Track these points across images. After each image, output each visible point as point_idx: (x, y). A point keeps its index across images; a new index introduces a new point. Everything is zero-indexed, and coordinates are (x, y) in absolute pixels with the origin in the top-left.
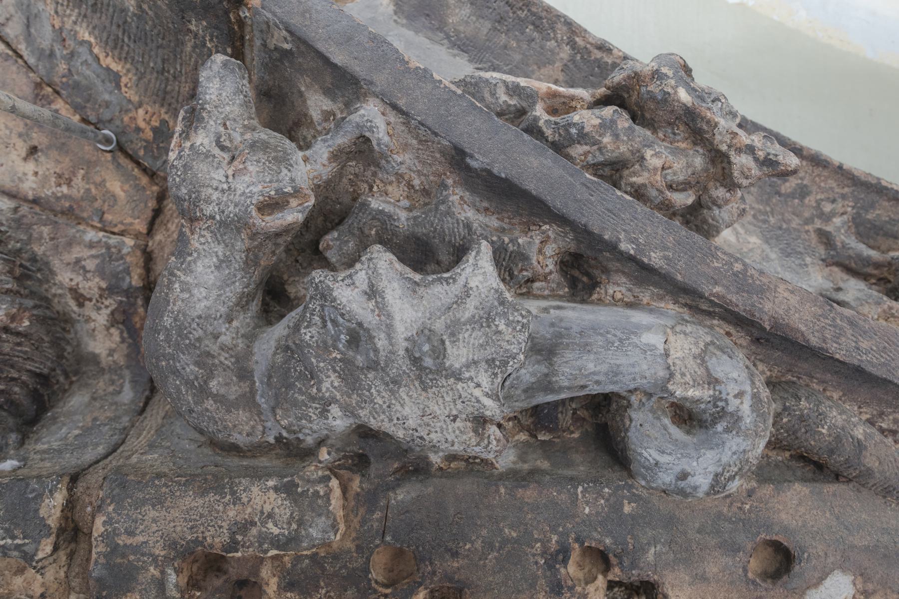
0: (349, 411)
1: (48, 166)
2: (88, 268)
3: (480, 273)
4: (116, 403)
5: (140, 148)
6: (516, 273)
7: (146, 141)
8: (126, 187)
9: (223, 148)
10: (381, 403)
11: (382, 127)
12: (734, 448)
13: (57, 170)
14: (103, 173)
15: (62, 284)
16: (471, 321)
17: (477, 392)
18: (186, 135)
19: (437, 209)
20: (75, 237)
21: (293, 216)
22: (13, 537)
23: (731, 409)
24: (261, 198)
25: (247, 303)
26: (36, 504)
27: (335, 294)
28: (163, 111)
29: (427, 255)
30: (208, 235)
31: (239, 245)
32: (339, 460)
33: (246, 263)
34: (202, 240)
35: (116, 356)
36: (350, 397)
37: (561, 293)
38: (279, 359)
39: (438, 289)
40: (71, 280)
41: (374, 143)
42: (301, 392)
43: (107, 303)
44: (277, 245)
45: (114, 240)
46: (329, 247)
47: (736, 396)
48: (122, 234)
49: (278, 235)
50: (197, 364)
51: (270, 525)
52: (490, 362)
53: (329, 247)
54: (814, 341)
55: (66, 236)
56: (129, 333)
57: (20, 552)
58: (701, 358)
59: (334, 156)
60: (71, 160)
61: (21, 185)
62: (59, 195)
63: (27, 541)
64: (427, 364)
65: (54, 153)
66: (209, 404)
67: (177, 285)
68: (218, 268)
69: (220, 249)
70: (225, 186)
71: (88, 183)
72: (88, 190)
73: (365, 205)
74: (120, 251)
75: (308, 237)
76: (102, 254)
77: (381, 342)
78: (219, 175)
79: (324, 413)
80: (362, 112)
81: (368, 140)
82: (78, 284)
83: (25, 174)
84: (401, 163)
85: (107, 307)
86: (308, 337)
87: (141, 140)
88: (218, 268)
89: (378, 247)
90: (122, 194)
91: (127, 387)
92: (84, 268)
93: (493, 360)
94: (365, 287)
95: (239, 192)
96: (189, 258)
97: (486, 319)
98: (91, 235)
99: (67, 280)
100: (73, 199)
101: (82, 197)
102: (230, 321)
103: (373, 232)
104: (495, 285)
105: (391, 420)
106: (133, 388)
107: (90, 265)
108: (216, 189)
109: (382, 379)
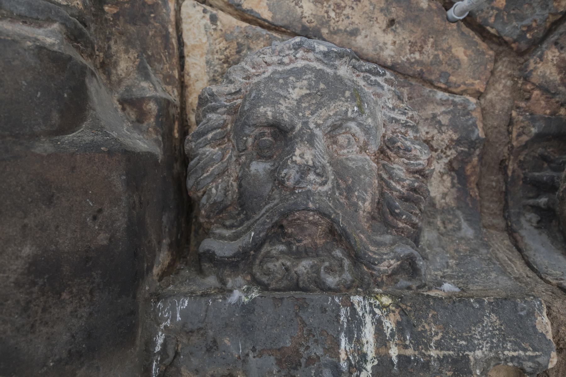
1: (404, 37)
2: (443, 122)
4: (462, 238)
5: (491, 16)
7: (497, 9)
8: (469, 52)
13: (412, 39)
14: (450, 41)
20: (429, 96)
22: (525, 350)
26: (531, 321)
35: (448, 199)
40: (427, 133)
43: (449, 153)
45: (458, 99)
48: (461, 93)
55: (421, 96)
56: (459, 179)
57: (534, 362)
60: (423, 30)
61: (381, 54)
62: (413, 60)
63: (537, 353)
65: (409, 25)
71: (436, 50)
72: (436, 56)
74: (465, 108)
76: (452, 111)
82: (433, 137)
83: (385, 44)
85: (449, 156)
87: (493, 8)
90: (465, 58)
91: (464, 225)
92: (439, 122)
98: (440, 95)
99: (424, 133)
100: (424, 64)
101: (431, 62)
106: (470, 226)
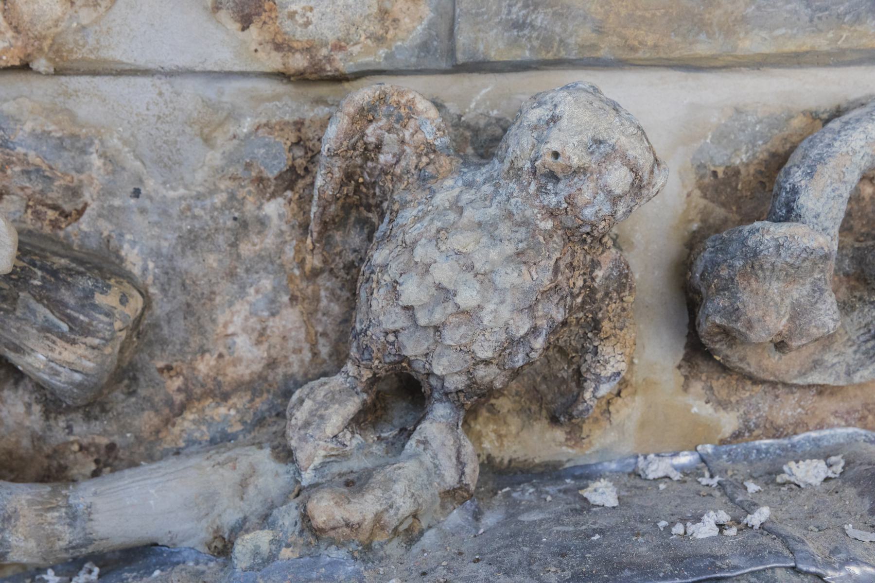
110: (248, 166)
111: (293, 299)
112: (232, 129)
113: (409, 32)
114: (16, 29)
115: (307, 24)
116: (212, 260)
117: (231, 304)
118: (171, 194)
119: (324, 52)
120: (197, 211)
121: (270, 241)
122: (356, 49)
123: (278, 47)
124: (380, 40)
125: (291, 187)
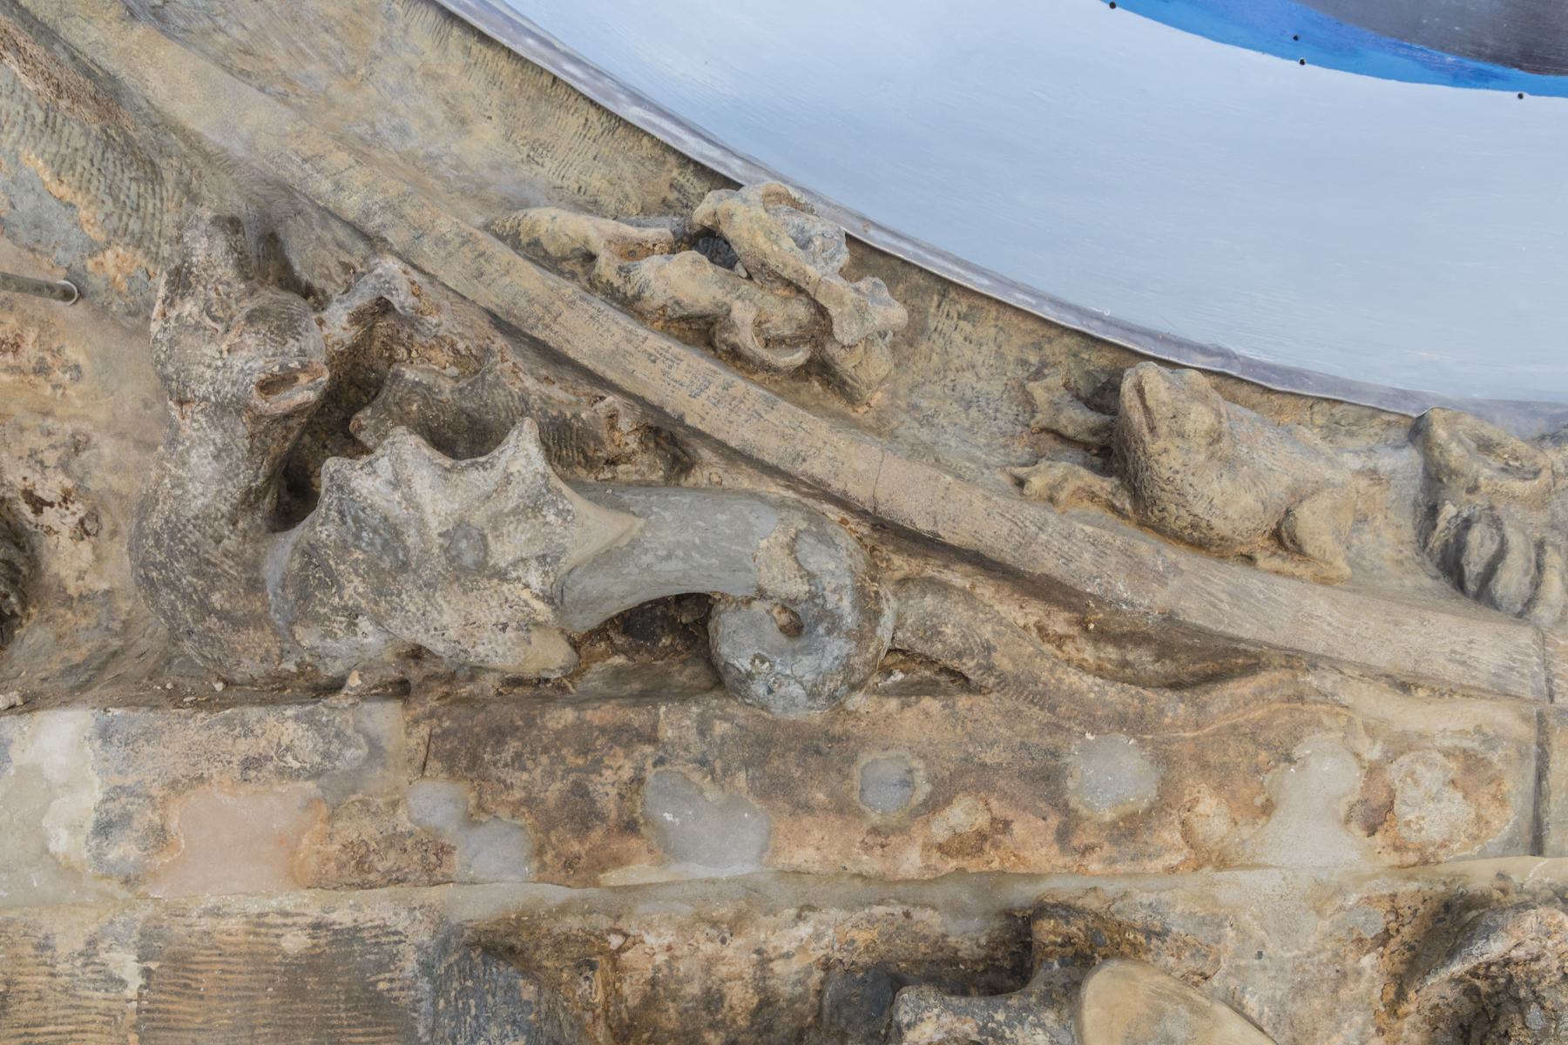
0: (378, 621)
3: (522, 454)
6: (590, 454)
9: (214, 319)
10: (413, 609)
11: (405, 286)
12: (836, 653)
15: (12, 484)
16: (514, 512)
17: (526, 595)
18: (169, 302)
19: (483, 378)
21: (303, 394)
23: (829, 606)
24: (263, 376)
25: (257, 499)
27: (353, 484)
28: (140, 252)
29: (463, 437)
30: (203, 420)
31: (241, 430)
32: (376, 687)
33: (251, 451)
34: (196, 425)
36: (376, 603)
37: (654, 477)
38: (296, 566)
39: (475, 475)
41: (397, 306)
42: (324, 605)
43: (73, 508)
44: (289, 429)
46: (361, 428)
47: (834, 591)
49: (287, 416)
50: (198, 574)
51: (289, 758)
52: (541, 559)
53: (361, 428)
54: (923, 525)
58: (792, 547)
59: (357, 318)
64: (467, 562)
66: (212, 622)
67: (167, 481)
68: (216, 457)
69: (217, 436)
70: (220, 363)
73: (398, 376)
75: (338, 415)
77: (412, 539)
78: (210, 350)
79: (352, 624)
80: (379, 271)
81: (388, 302)
84: (438, 325)
85: (74, 514)
86: (324, 536)
88: (216, 457)
89: (402, 429)
92: (41, 463)
93: (544, 556)
94: (389, 475)
95: (236, 370)
96: (180, 448)
97: (533, 507)
102: (235, 524)
103: (414, 408)
104: (541, 470)
105: (427, 631)
107: (51, 458)
108: (209, 366)
109: (414, 582)
110: (1351, 931)
111: (1381, 1031)
112: (1339, 902)
113: (1498, 830)
114: (1192, 847)
115: (1421, 830)
116: (1316, 1003)
117: (1329, 1037)
118: (1288, 955)
119: (1431, 849)
120: (1307, 967)
121: (1363, 986)
122: (1456, 846)
123: (1397, 849)
124: (1475, 838)
125: (1384, 944)
